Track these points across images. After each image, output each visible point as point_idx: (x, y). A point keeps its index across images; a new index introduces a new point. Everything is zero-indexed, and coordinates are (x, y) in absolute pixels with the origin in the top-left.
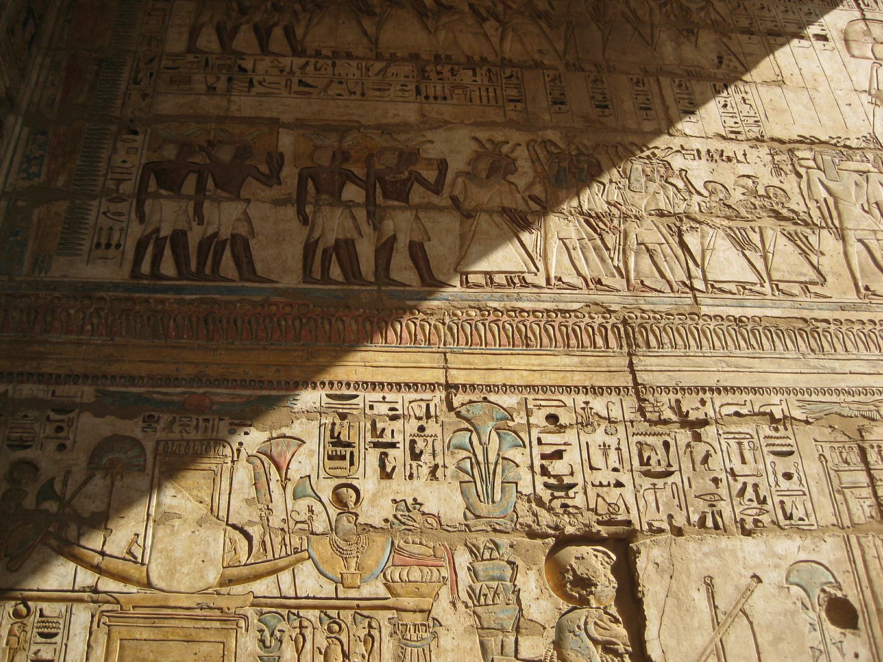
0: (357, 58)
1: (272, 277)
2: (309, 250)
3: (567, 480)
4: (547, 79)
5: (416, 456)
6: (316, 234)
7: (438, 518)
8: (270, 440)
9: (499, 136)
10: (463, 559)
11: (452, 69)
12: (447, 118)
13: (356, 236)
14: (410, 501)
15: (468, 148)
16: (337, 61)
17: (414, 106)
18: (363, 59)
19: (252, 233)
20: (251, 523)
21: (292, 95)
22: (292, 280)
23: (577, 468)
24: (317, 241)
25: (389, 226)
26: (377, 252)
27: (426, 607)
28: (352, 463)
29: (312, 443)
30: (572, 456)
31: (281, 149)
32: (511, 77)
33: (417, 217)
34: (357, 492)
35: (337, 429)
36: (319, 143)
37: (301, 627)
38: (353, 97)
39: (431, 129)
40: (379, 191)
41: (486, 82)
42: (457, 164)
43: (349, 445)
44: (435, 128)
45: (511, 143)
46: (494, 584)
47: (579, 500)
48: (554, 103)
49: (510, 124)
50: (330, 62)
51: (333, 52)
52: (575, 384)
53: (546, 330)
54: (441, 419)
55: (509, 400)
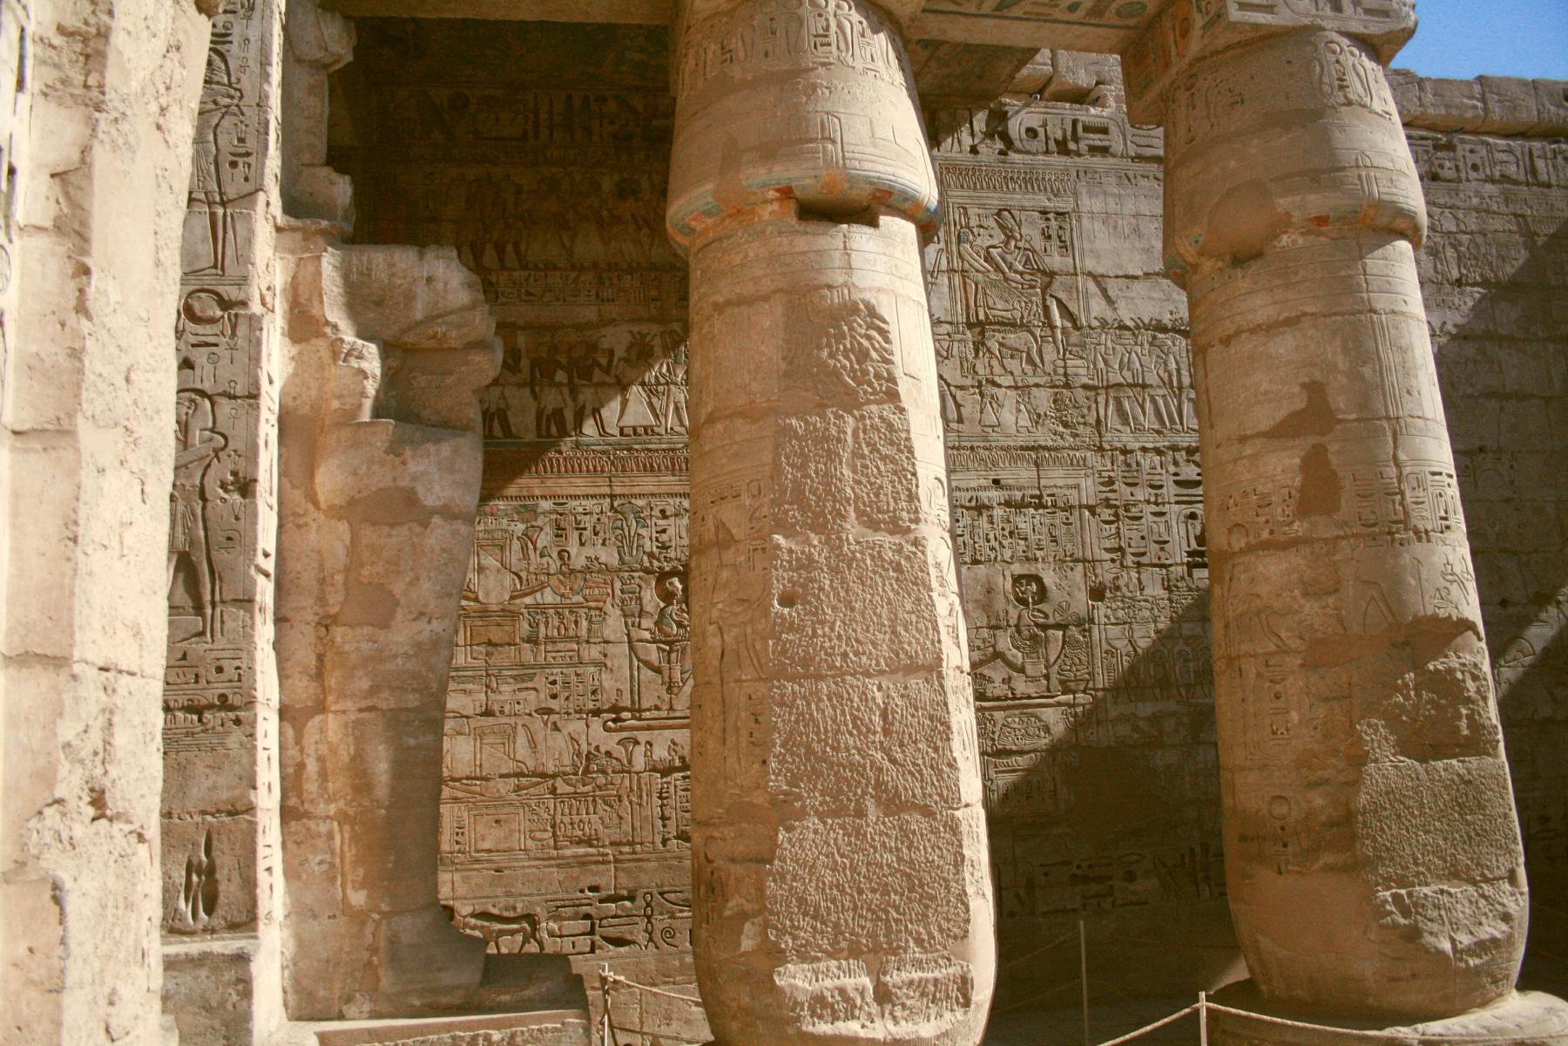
2: (539, 414)
5: (596, 534)
9: (644, 328)
10: (618, 585)
15: (626, 339)
17: (594, 309)
18: (565, 270)
19: (508, 407)
22: (530, 437)
25: (581, 397)
26: (575, 415)
29: (547, 529)
30: (671, 531)
39: (604, 326)
42: (620, 352)
47: (672, 554)
49: (651, 320)
55: (641, 502)
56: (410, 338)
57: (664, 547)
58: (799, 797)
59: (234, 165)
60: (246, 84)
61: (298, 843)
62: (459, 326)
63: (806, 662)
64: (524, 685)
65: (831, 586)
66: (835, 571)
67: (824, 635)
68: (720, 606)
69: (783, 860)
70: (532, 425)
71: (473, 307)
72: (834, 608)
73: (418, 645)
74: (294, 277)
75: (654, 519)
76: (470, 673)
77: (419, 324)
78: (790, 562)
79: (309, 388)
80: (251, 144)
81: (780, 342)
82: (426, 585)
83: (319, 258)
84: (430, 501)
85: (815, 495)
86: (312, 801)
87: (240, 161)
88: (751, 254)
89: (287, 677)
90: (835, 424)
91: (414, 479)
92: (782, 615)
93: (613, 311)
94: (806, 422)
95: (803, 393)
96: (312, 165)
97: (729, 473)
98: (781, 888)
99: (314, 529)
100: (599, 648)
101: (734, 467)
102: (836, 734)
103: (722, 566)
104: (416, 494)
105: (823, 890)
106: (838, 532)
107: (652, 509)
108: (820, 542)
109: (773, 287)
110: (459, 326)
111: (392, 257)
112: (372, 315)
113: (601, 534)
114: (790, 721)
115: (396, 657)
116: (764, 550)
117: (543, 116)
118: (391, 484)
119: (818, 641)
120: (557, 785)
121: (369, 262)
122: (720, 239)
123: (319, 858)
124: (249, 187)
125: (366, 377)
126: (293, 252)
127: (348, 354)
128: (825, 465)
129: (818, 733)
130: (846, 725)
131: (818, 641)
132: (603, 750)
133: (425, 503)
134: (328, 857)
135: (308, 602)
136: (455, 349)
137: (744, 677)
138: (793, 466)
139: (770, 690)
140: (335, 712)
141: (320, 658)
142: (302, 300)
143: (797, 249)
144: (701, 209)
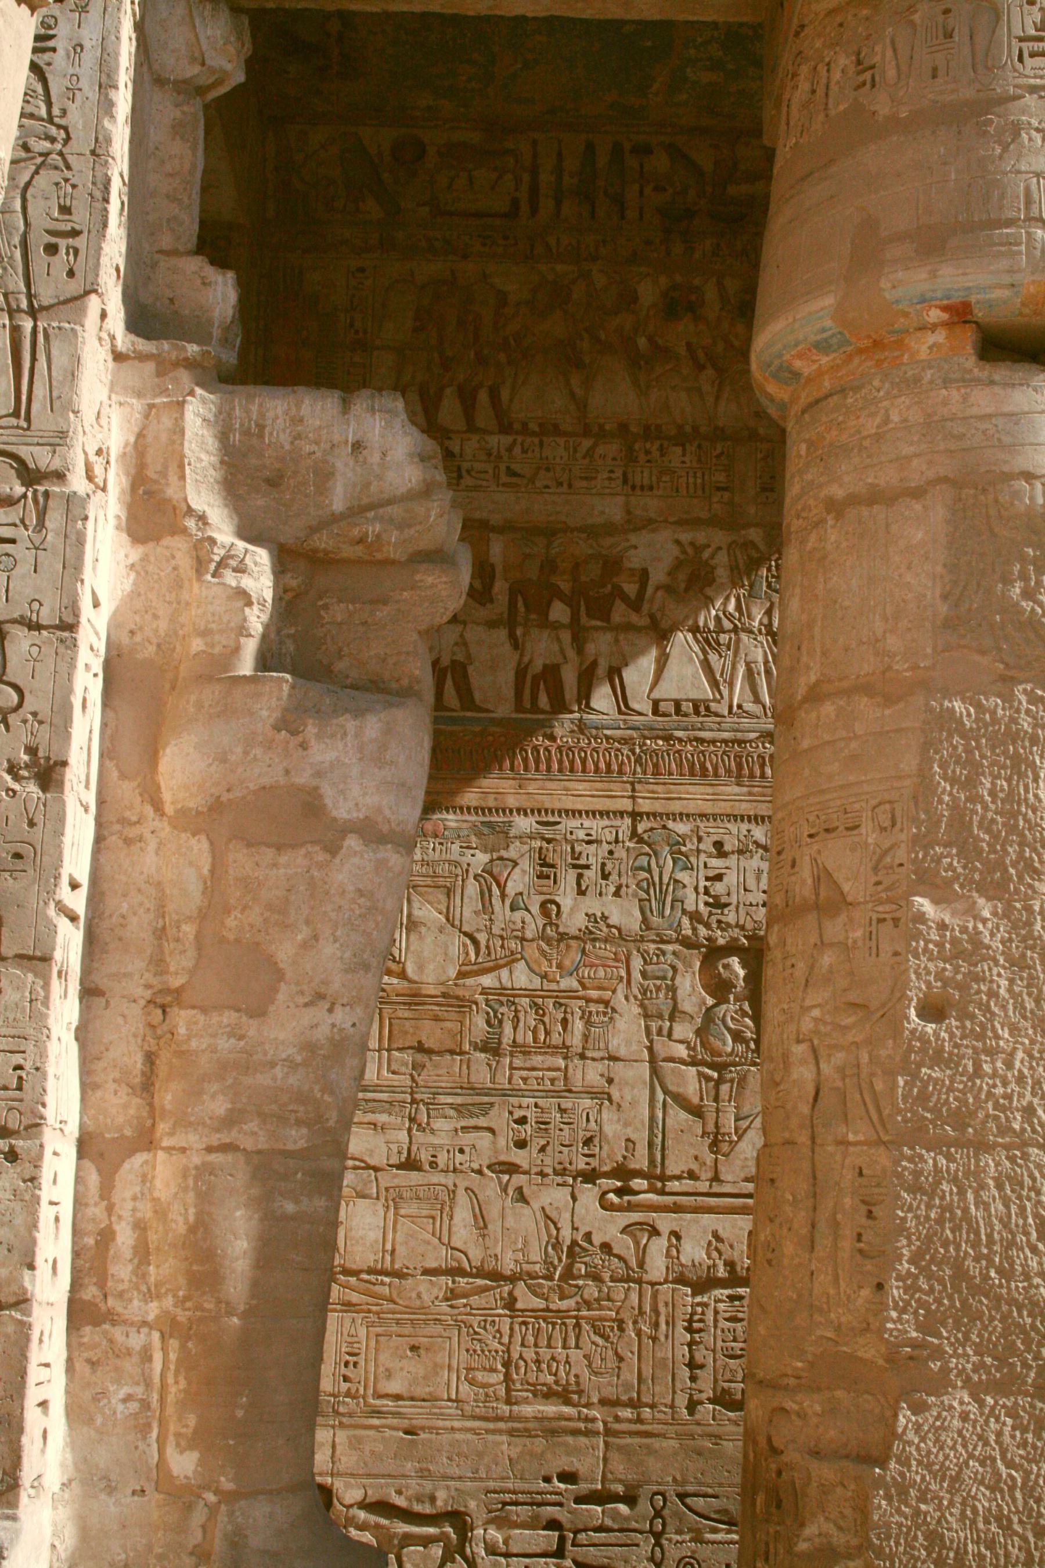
0: (565, 434)
1: (490, 706)
2: (521, 674)
3: (723, 900)
4: (759, 456)
5: (605, 876)
6: (526, 659)
7: (619, 930)
8: (492, 861)
9: (701, 537)
10: (637, 963)
11: (661, 445)
12: (652, 515)
13: (561, 661)
14: (599, 914)
15: (669, 553)
16: (545, 439)
17: (620, 500)
19: (469, 656)
20: (478, 930)
21: (501, 489)
22: (504, 710)
23: (734, 890)
24: (527, 667)
25: (591, 648)
26: (580, 677)
27: (607, 998)
28: (555, 882)
29: (525, 864)
30: (731, 879)
31: (493, 560)
32: (722, 453)
33: (617, 640)
34: (558, 906)
35: (544, 851)
36: (527, 551)
37: (516, 1011)
38: (560, 490)
39: (636, 529)
40: (583, 608)
41: (695, 464)
42: (658, 575)
43: (552, 866)
44: (639, 529)
45: (714, 546)
46: (658, 982)
47: (731, 917)
48: (764, 489)
49: (713, 522)
50: (536, 440)
51: (541, 425)
52: (742, 812)
53: (723, 761)
54: (628, 844)
55: (682, 828)
56: (322, 541)
57: (718, 904)
58: (938, 1353)
59: (52, 249)
60: (75, 119)
61: (93, 1364)
62: (402, 526)
63: (960, 1119)
64: (472, 1122)
65: (1010, 990)
66: (1018, 964)
67: (994, 1075)
68: (816, 1013)
69: (905, 1462)
70: (509, 692)
71: (427, 491)
72: (1014, 1029)
73: (310, 1047)
74: (140, 436)
75: (703, 857)
76: (384, 1096)
77: (336, 518)
78: (940, 945)
79: (156, 617)
80: (80, 218)
81: (939, 569)
82: (328, 949)
83: (181, 404)
84: (342, 811)
85: (988, 831)
86: (121, 1295)
87: (62, 243)
88: (895, 417)
89: (96, 1087)
90: (1028, 712)
91: (319, 774)
92: (924, 1033)
93: (650, 505)
94: (979, 706)
95: (977, 658)
96: (173, 253)
97: (842, 787)
98: (898, 1511)
99: (152, 846)
100: (601, 1067)
101: (852, 778)
102: (1008, 1248)
103: (822, 945)
104: (321, 797)
105: (974, 1522)
106: (1027, 898)
107: (700, 840)
108: (995, 914)
109: (930, 474)
110: (402, 526)
111: (298, 406)
112: (260, 502)
113: (614, 877)
114: (927, 1218)
115: (273, 1064)
116: (896, 921)
117: (546, 177)
118: (282, 781)
119: (984, 1084)
120: (517, 1293)
121: (262, 415)
122: (843, 391)
123: (122, 1393)
124: (74, 287)
125: (249, 604)
126: (139, 395)
127: (220, 564)
128: (1009, 780)
129: (976, 1244)
130: (1027, 1234)
131: (984, 1084)
132: (597, 1240)
133: (334, 813)
134: (139, 1391)
135: (136, 965)
136: (393, 562)
137: (851, 1137)
138: (953, 781)
139: (897, 1162)
140: (168, 1150)
141: (150, 1058)
142: (151, 474)
143: (975, 411)
144: (813, 338)
